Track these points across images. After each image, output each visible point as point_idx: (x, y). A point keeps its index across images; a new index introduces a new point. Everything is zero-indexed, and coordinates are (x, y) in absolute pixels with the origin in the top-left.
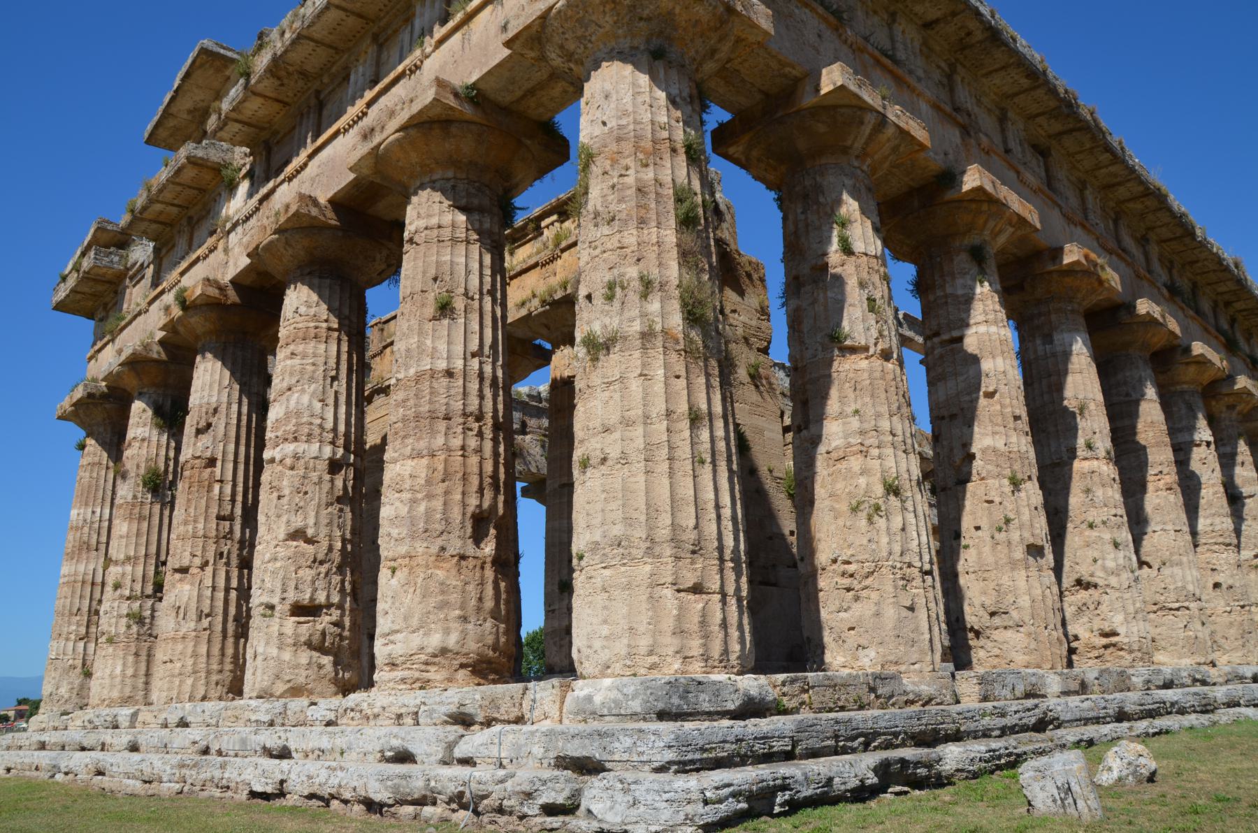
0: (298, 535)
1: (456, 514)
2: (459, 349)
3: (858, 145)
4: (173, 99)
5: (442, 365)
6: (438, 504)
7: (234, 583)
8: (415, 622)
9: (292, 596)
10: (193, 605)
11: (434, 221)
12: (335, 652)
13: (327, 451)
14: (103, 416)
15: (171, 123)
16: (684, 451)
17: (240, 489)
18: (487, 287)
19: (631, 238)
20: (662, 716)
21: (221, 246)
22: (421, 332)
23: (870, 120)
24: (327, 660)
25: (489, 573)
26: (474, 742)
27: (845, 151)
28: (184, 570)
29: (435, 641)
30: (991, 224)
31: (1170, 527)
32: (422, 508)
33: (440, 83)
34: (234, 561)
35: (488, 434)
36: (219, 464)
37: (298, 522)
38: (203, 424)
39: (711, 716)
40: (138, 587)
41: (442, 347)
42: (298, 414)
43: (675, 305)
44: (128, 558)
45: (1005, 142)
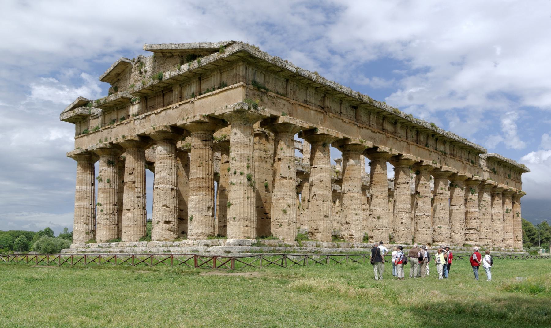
0: (165, 205)
1: (204, 207)
2: (204, 173)
3: (291, 131)
5: (201, 177)
8: (196, 227)
9: (164, 219)
10: (132, 218)
11: (198, 143)
12: (174, 232)
13: (171, 187)
14: (87, 159)
16: (246, 203)
20: (240, 245)
23: (293, 126)
24: (172, 233)
26: (210, 249)
27: (287, 132)
28: (129, 210)
29: (200, 231)
30: (327, 139)
37: (165, 203)
38: (131, 172)
39: (247, 245)
40: (108, 211)
43: (246, 178)
45: (341, 110)
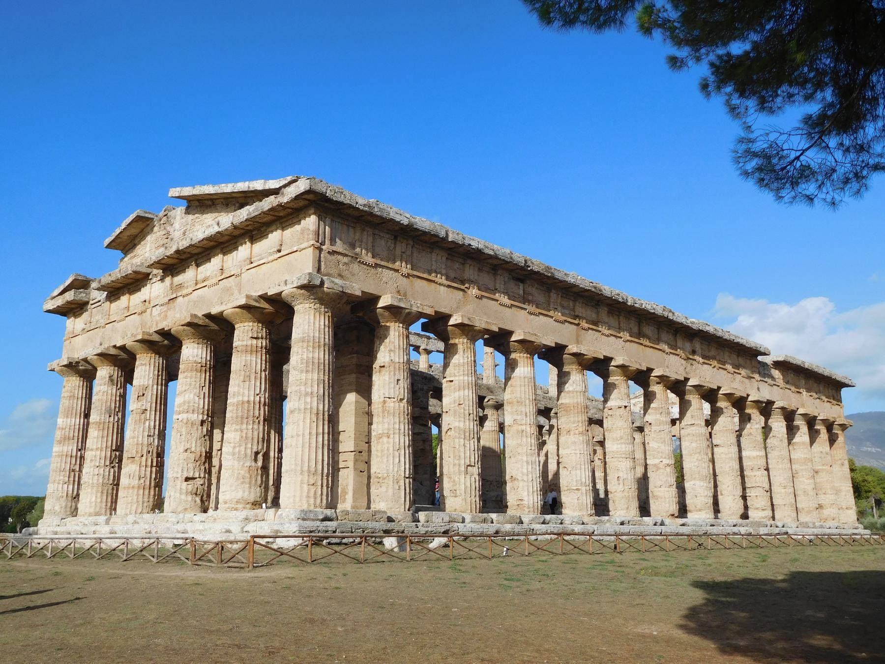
1: (249, 451)
4: (121, 232)
5: (246, 399)
6: (243, 448)
7: (155, 464)
10: (137, 473)
11: (245, 343)
15: (119, 240)
17: (157, 423)
18: (263, 368)
19: (304, 376)
21: (149, 311)
22: (239, 386)
25: (260, 472)
29: (239, 495)
31: (578, 452)
32: (237, 449)
33: (248, 297)
34: (155, 455)
35: (262, 423)
36: (148, 412)
41: (246, 393)
42: (189, 402)
44: (97, 449)
